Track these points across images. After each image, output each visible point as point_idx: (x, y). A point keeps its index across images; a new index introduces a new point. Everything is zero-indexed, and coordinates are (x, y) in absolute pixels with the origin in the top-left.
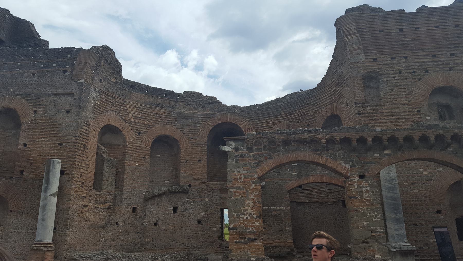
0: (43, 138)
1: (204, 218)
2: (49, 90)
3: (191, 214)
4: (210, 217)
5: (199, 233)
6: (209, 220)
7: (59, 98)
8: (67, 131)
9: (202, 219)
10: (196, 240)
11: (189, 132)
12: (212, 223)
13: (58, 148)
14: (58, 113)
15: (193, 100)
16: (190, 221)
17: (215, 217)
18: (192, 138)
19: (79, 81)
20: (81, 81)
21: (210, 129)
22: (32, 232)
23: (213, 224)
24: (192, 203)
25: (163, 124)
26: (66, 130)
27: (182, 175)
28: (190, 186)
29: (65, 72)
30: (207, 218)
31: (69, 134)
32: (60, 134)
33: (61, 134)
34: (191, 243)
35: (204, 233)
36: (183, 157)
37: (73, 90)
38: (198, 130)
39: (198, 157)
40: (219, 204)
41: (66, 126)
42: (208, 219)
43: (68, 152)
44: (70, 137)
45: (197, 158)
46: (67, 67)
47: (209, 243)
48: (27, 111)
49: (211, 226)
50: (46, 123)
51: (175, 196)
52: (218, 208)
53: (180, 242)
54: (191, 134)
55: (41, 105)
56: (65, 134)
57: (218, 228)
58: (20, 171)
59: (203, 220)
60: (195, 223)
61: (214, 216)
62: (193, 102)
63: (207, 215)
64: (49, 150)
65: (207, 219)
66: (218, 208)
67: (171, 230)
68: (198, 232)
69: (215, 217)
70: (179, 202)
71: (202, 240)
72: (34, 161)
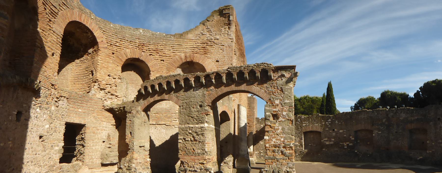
1: (48, 132)
4: (54, 132)
5: (39, 154)
6: (53, 135)
9: (45, 134)
10: (35, 164)
12: (55, 141)
16: (32, 136)
17: (59, 133)
23: (55, 142)
30: (51, 133)
34: (30, 170)
35: (46, 153)
40: (65, 116)
42: (52, 134)
47: (49, 167)
49: (54, 144)
52: (63, 121)
57: (60, 147)
61: (58, 131)
63: (52, 129)
65: (50, 135)
66: (63, 121)
68: (39, 153)
69: (59, 133)
71: (42, 164)
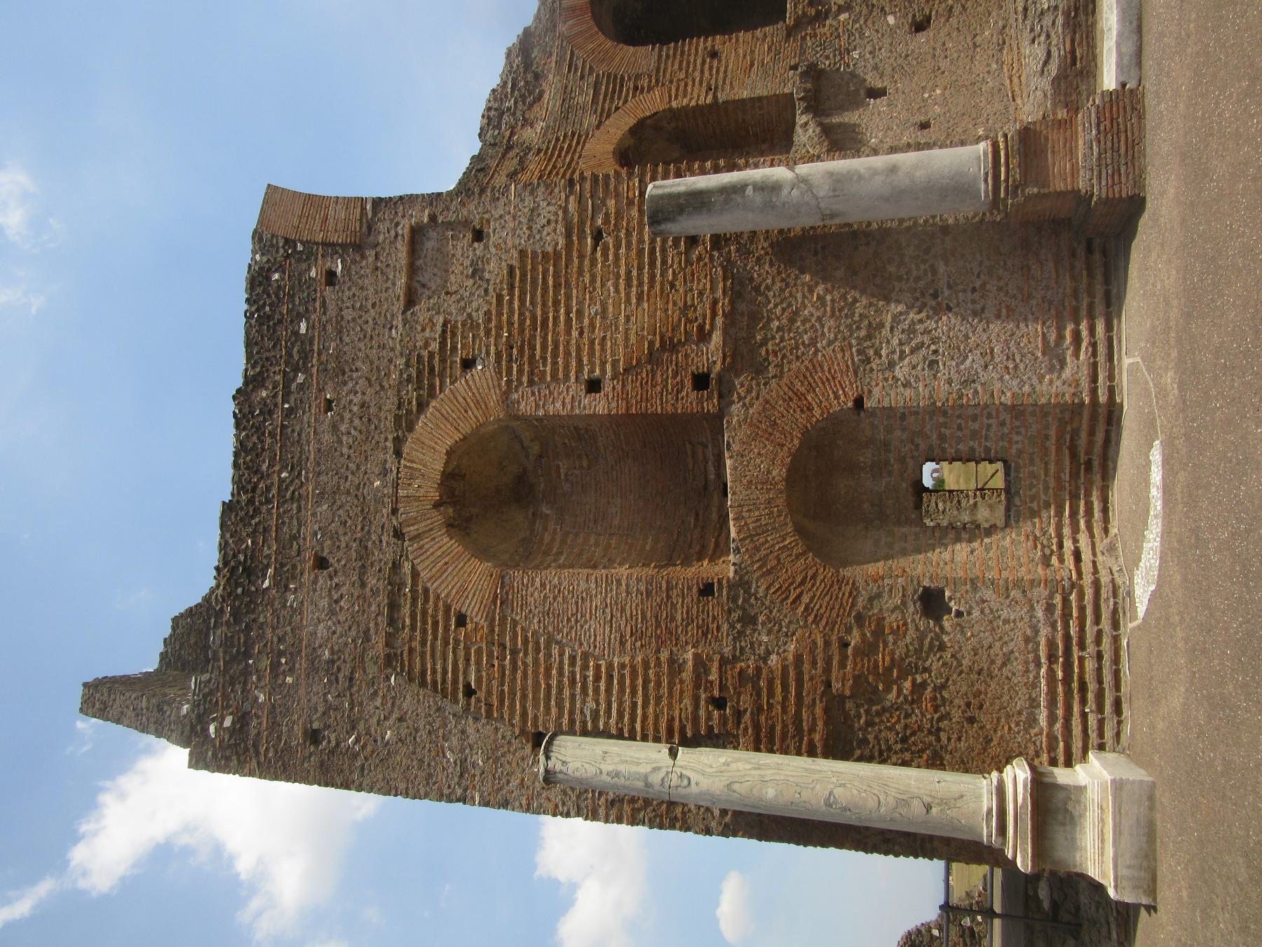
0: (568, 313)
2: (391, 329)
3: (891, 51)
7: (424, 286)
8: (549, 222)
10: (981, 25)
11: (612, 98)
13: (610, 241)
14: (479, 273)
15: (509, 109)
18: (636, 88)
19: (370, 216)
20: (368, 207)
21: (609, 43)
22: (945, 289)
24: (855, 55)
25: (579, 157)
26: (543, 227)
27: (757, 92)
28: (794, 68)
29: (331, 277)
31: (560, 213)
32: (560, 247)
33: (557, 244)
36: (698, 99)
37: (400, 232)
38: (609, 77)
39: (699, 61)
41: (530, 228)
43: (630, 203)
44: (572, 206)
45: (704, 63)
46: (313, 274)
48: (461, 400)
50: (511, 311)
51: (829, 99)
53: (988, 65)
54: (621, 91)
55: (443, 344)
56: (561, 228)
58: (693, 390)
59: (914, 16)
60: (922, 38)
62: (516, 107)
63: (896, 6)
64: (618, 276)
67: (947, 92)
70: (848, 87)
72: (655, 334)
